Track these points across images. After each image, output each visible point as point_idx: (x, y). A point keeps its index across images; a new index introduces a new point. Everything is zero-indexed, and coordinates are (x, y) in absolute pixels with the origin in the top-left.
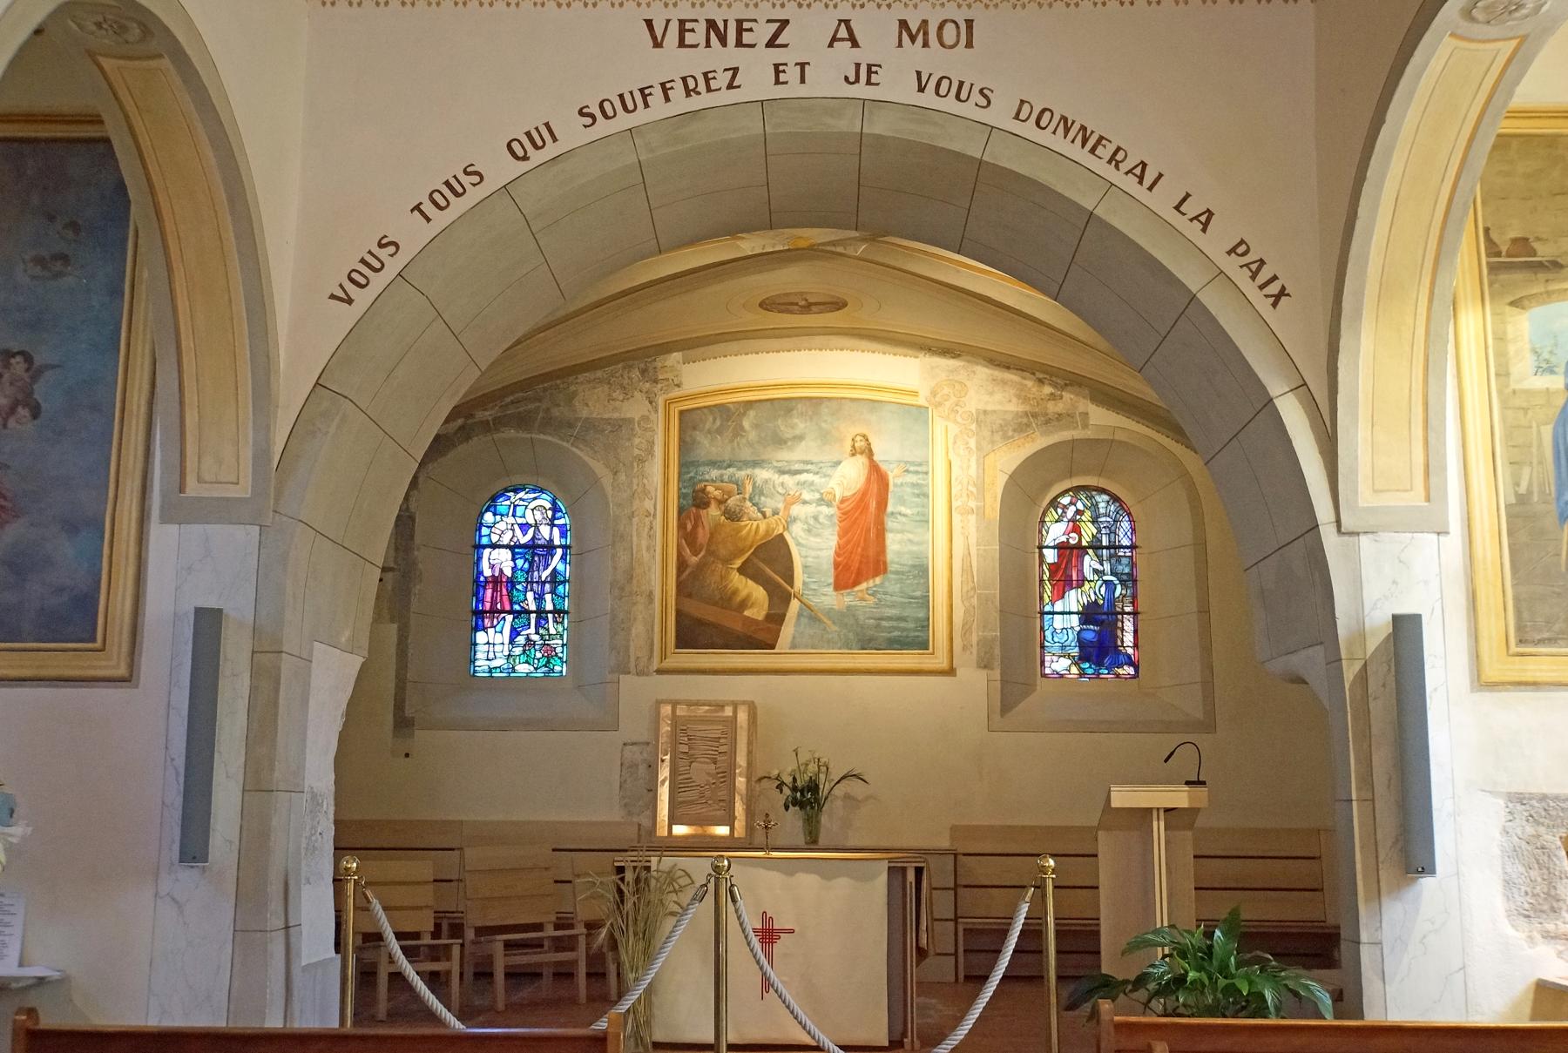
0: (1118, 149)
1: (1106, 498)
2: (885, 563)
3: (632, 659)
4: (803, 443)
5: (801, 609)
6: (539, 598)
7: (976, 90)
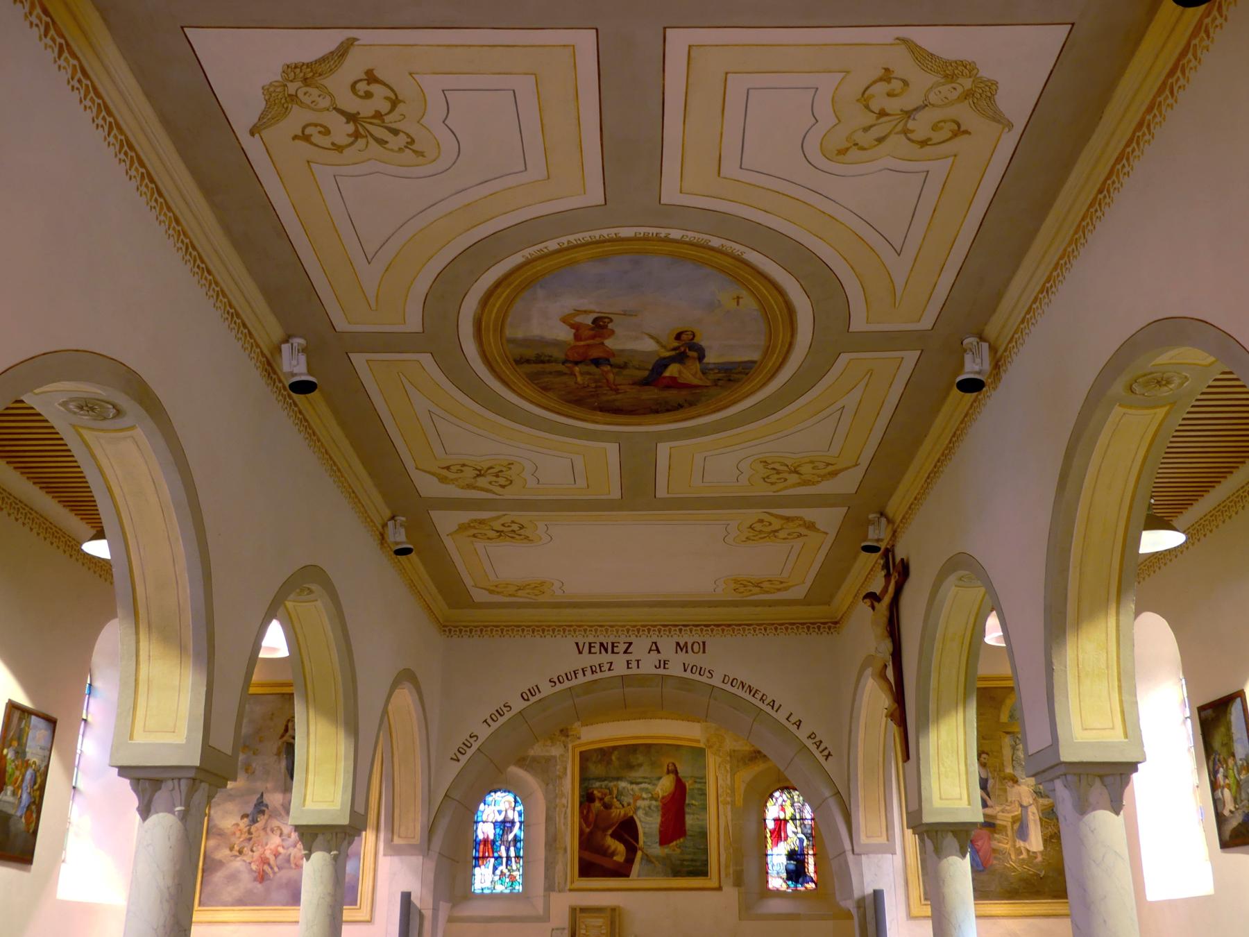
0: (764, 695)
1: (797, 793)
2: (685, 830)
3: (557, 884)
4: (642, 768)
5: (642, 855)
6: (508, 850)
7: (707, 671)
